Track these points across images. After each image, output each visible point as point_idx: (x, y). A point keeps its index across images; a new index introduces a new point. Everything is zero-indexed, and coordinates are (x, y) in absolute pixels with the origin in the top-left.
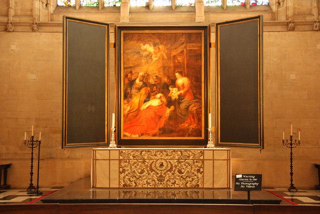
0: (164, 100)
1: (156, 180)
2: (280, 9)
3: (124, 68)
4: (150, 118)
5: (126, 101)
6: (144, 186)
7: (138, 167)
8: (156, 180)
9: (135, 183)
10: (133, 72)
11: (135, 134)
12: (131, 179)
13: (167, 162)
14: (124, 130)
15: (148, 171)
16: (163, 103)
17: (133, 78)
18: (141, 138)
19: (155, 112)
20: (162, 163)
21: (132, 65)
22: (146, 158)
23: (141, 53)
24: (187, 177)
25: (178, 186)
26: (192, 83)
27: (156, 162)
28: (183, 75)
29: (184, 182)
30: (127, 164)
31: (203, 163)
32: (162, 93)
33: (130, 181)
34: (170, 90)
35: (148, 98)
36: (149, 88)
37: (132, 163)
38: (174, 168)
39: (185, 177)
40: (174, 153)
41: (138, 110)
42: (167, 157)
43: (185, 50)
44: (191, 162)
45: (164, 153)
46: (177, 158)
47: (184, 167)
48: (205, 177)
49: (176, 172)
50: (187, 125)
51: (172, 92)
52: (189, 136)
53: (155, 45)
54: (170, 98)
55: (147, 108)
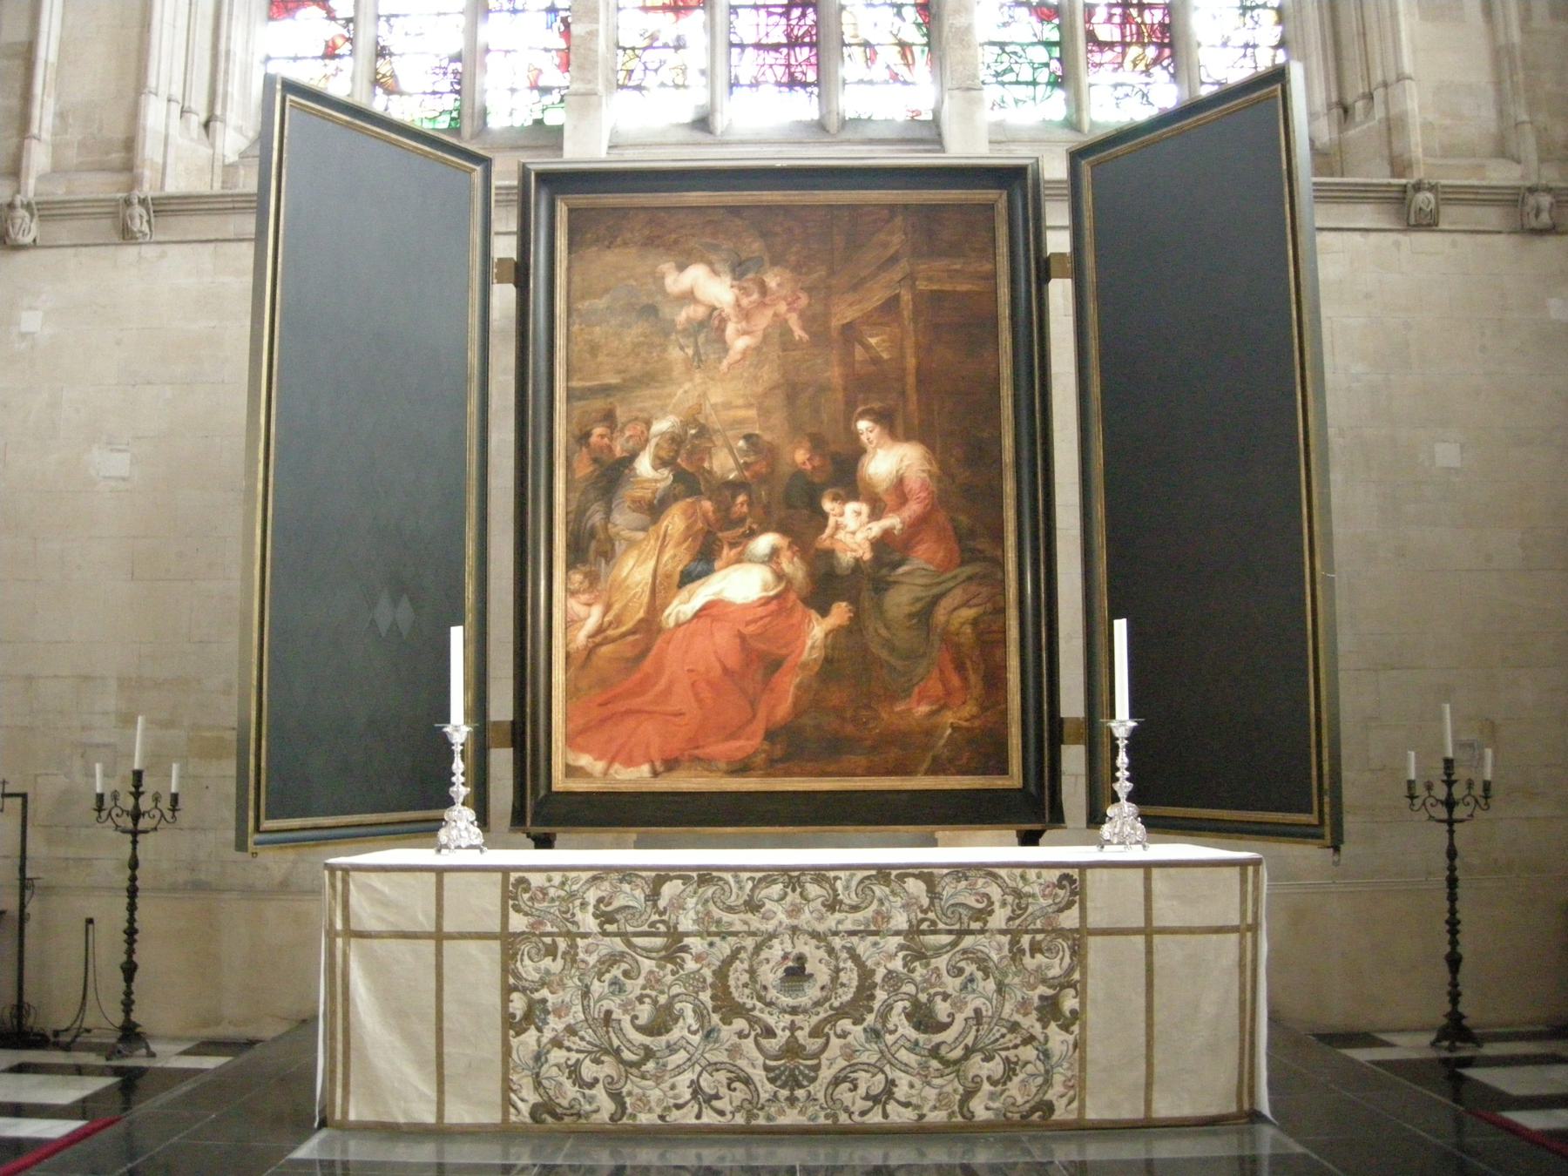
0: (793, 567)
1: (758, 1075)
3: (571, 395)
4: (718, 671)
5: (577, 577)
6: (675, 1117)
7: (634, 987)
8: (758, 1075)
9: (616, 1097)
10: (621, 414)
11: (630, 762)
12: (588, 1070)
13: (831, 951)
14: (570, 741)
15: (700, 1014)
16: (790, 582)
17: (619, 451)
18: (665, 784)
19: (742, 638)
20: (801, 959)
21: (614, 380)
22: (686, 923)
23: (666, 311)
24: (969, 1052)
25: (907, 1116)
26: (952, 477)
27: (758, 949)
28: (900, 430)
29: (954, 1087)
30: (556, 966)
31: (1078, 952)
32: (782, 529)
33: (578, 1079)
34: (825, 516)
35: (703, 560)
36: (707, 505)
37: (592, 960)
38: (881, 995)
39: (958, 1053)
40: (879, 890)
41: (650, 626)
42: (831, 921)
43: (906, 297)
44: (994, 948)
45: (813, 890)
46: (900, 921)
47: (952, 984)
48: (1090, 1056)
49: (897, 1019)
50: (923, 709)
51: (838, 527)
52: (936, 769)
53: (739, 269)
54: (830, 554)
55: (698, 615)
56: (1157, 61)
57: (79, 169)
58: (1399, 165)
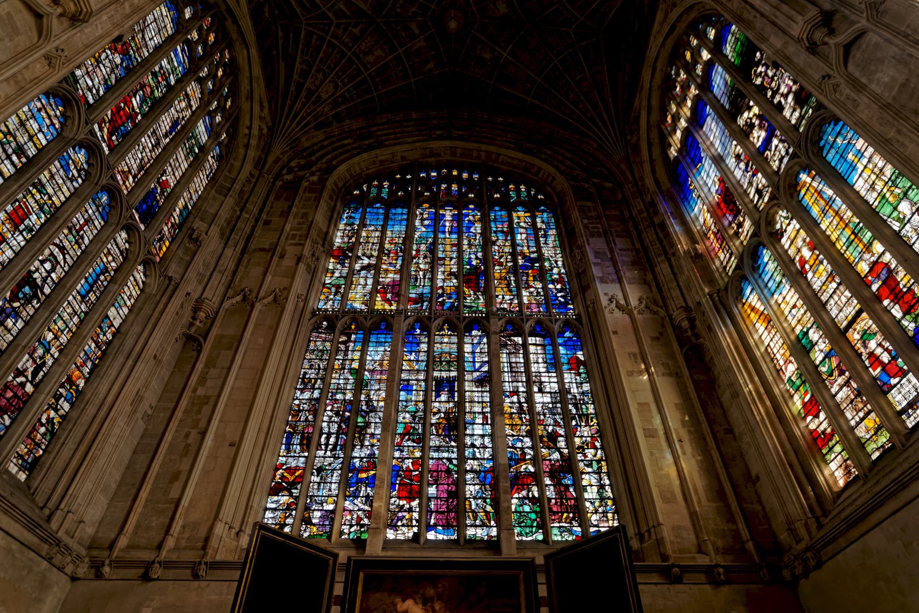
2: (645, 545)
56: (573, 519)
57: (185, 548)
58: (664, 557)
